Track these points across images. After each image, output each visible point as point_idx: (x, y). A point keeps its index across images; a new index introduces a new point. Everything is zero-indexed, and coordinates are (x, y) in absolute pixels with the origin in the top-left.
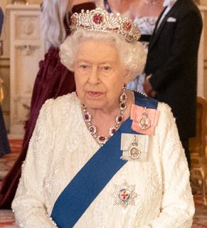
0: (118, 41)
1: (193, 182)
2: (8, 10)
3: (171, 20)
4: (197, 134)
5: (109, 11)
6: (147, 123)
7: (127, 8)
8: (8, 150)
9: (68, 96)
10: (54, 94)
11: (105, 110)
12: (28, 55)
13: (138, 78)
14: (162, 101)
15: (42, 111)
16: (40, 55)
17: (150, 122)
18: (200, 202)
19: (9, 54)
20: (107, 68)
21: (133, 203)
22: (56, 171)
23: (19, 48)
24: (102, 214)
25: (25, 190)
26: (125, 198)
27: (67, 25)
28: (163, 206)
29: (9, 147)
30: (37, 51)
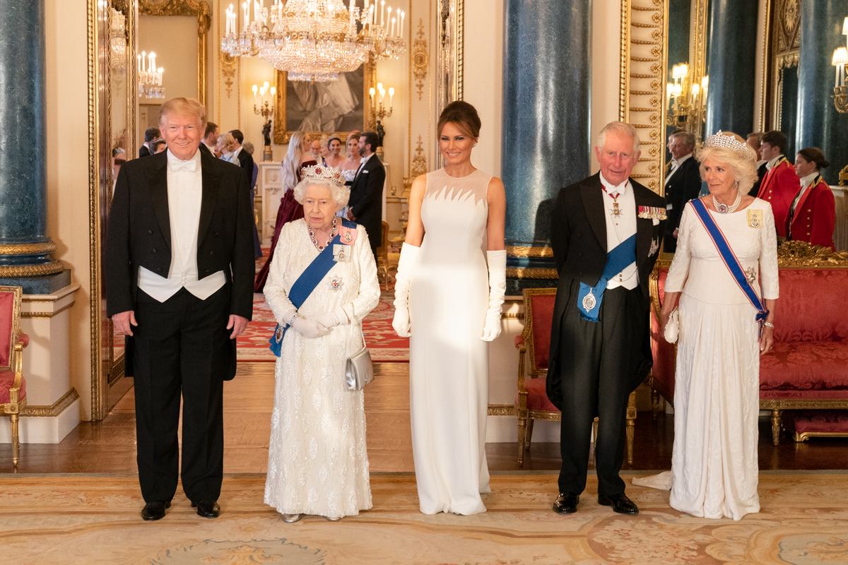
0: (331, 185)
1: (379, 275)
2: (261, 166)
3: (365, 172)
4: (382, 245)
5: (326, 166)
6: (350, 237)
7: (337, 164)
8: (261, 255)
9: (299, 221)
10: (290, 219)
11: (323, 229)
12: (274, 194)
13: (344, 209)
14: (359, 224)
15: (282, 230)
16: (281, 194)
17: (352, 237)
18: (384, 288)
19: (261, 193)
20: (324, 203)
21: (341, 289)
22: (292, 269)
23: (268, 190)
24: (321, 296)
25: (272, 280)
26: (336, 285)
27: (299, 175)
28: (361, 290)
29: (261, 253)
30: (279, 192)
